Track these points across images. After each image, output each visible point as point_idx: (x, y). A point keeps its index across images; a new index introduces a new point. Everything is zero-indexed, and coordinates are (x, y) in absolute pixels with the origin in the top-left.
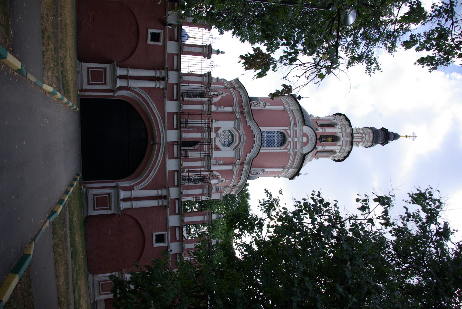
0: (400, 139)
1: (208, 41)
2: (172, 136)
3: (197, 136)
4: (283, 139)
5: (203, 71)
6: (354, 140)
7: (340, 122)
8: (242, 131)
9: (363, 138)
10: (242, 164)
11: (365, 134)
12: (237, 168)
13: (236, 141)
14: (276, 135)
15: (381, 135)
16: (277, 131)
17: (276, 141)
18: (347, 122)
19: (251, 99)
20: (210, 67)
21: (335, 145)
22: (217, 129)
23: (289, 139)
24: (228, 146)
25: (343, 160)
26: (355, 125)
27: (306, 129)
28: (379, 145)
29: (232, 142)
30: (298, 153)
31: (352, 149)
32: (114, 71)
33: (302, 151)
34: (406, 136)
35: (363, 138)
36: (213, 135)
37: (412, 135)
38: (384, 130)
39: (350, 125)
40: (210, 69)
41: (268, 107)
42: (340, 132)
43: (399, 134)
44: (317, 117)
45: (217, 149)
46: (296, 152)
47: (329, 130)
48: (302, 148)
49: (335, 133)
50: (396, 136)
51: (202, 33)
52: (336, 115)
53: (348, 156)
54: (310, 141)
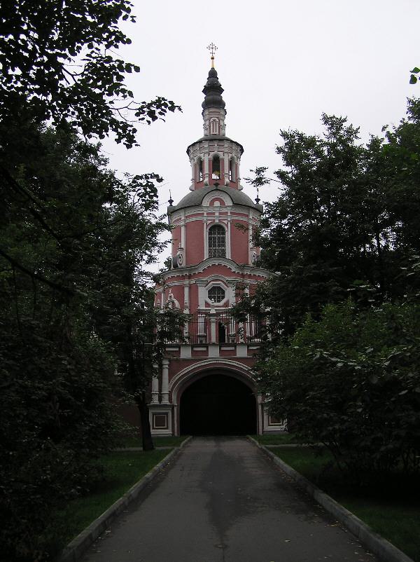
2: (214, 353)
3: (213, 328)
4: (217, 229)
10: (243, 276)
13: (219, 284)
16: (209, 234)
18: (198, 145)
21: (223, 160)
22: (207, 304)
23: (217, 221)
24: (223, 292)
27: (206, 203)
31: (228, 140)
32: (155, 406)
34: (213, 58)
36: (213, 311)
38: (206, 90)
41: (183, 246)
47: (206, 170)
48: (226, 207)
50: (213, 74)
52: (188, 154)
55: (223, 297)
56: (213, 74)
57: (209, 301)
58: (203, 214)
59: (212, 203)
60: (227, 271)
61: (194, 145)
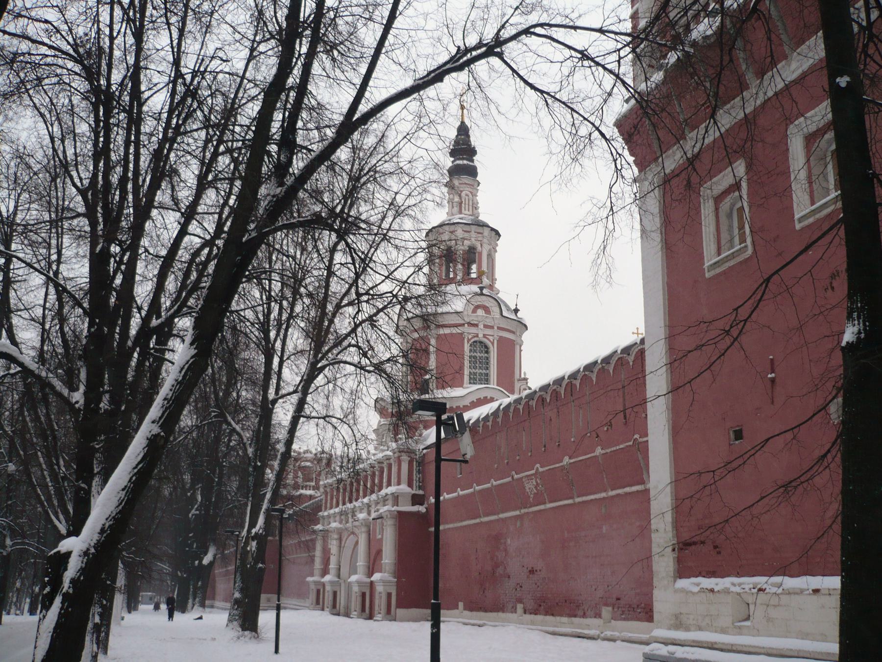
21: (480, 254)
46: (498, 328)
50: (463, 130)
56: (463, 130)
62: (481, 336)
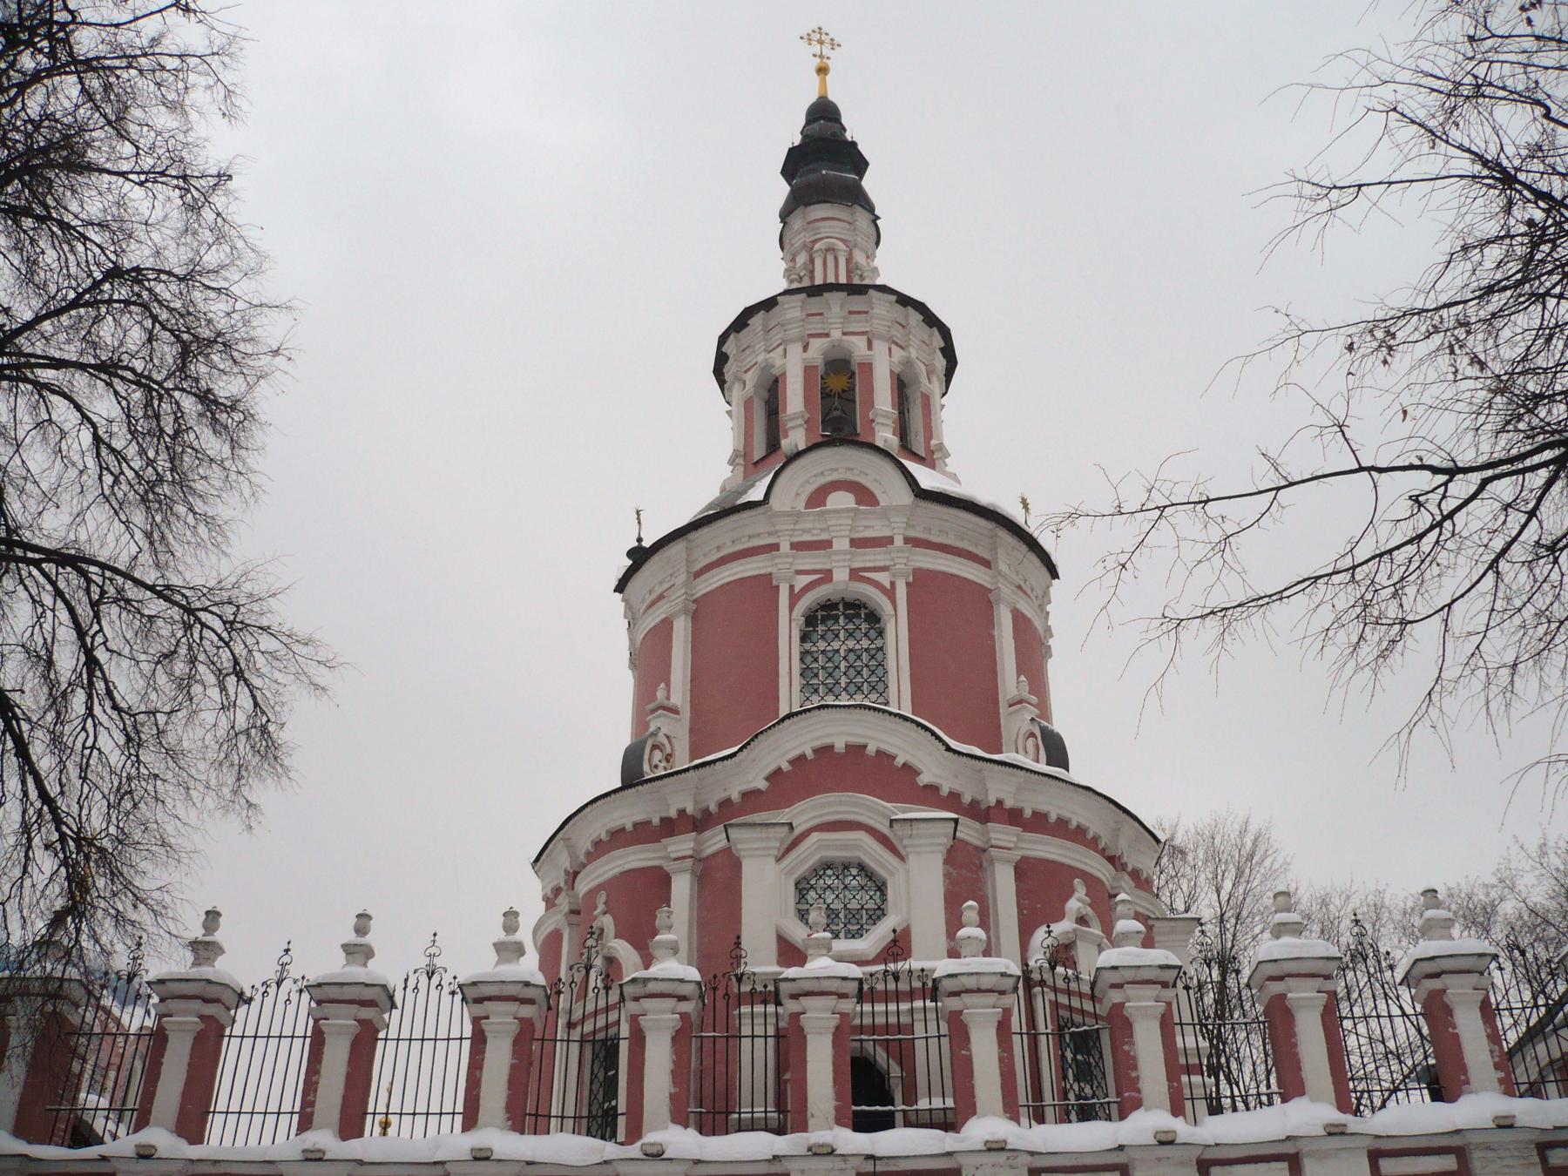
0: (832, 97)
1: (292, 1008)
5: (455, 1033)
6: (843, 280)
7: (755, 353)
8: (803, 813)
9: (831, 249)
11: (815, 242)
12: (1001, 834)
14: (822, 645)
15: (813, 177)
16: (804, 638)
17: (851, 644)
18: (756, 321)
19: (632, 776)
20: (434, 993)
21: (868, 367)
24: (881, 888)
25: (945, 333)
26: (773, 281)
28: (869, 183)
29: (862, 867)
30: (912, 533)
33: (898, 509)
35: (831, 249)
37: (816, 48)
38: (795, 164)
39: (769, 304)
40: (446, 990)
42: (805, 348)
43: (813, 98)
44: (732, 462)
45: (898, 947)
46: (907, 540)
47: (794, 401)
48: (885, 515)
49: (808, 370)
51: (248, 1043)
52: (721, 382)
53: (920, 307)
54: (851, 477)
55: (878, 913)
57: (797, 933)
58: (775, 547)
59: (817, 498)
60: (895, 780)
61: (740, 323)
62: (841, 575)
